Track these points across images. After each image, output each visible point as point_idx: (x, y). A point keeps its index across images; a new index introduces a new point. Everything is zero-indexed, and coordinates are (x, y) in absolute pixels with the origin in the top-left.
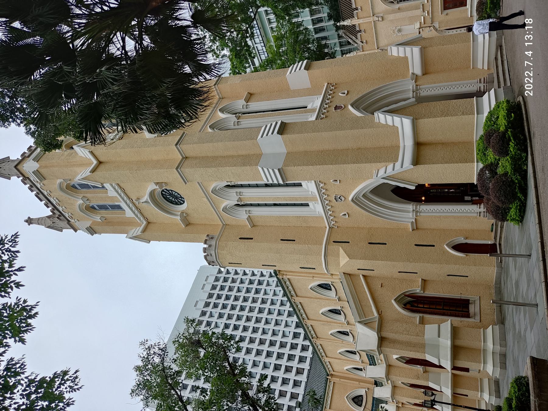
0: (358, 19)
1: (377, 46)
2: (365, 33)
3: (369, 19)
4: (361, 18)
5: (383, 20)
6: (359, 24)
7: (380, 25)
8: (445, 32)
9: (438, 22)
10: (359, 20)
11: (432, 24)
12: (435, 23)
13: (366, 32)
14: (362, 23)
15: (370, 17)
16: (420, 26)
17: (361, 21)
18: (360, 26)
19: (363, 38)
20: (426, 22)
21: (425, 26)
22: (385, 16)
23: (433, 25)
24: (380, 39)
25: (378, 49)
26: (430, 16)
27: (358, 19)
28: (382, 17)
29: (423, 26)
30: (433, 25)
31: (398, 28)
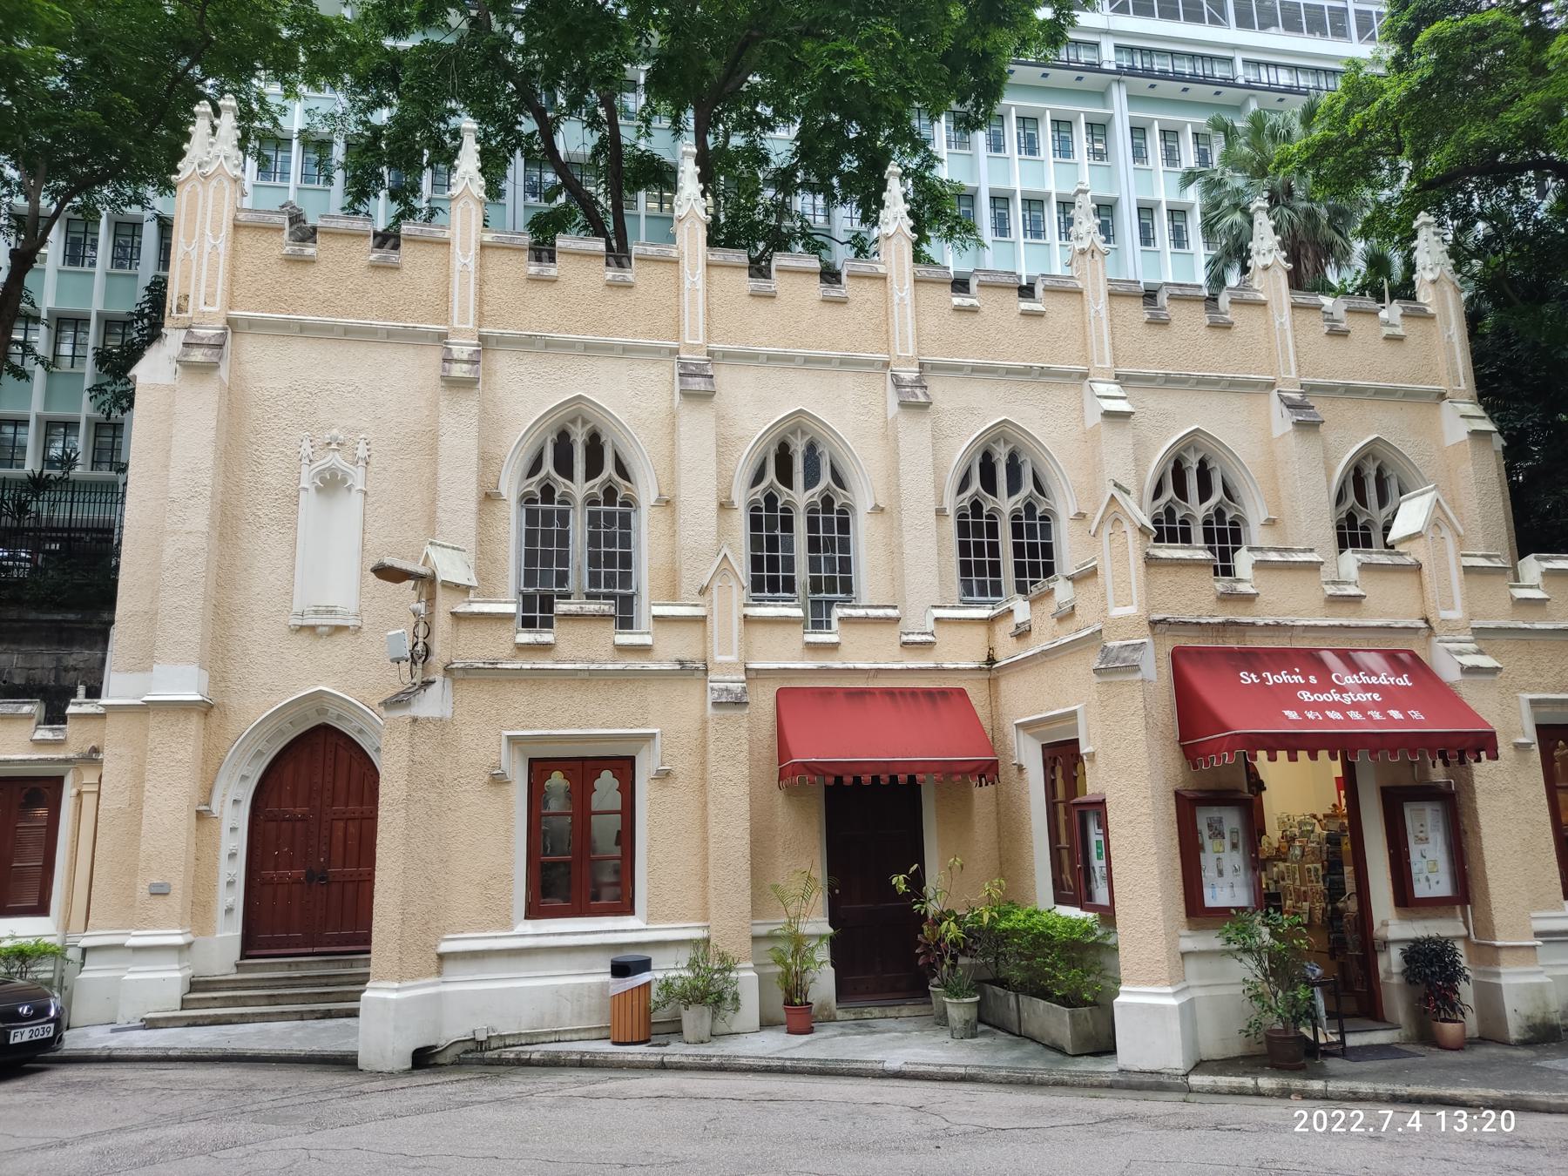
0: (483, 247)
1: (252, 324)
2: (375, 267)
3: (464, 311)
4: (481, 267)
5: (453, 384)
6: (447, 243)
7: (420, 367)
8: (244, 778)
9: (449, 715)
10: (474, 248)
11: (448, 670)
12: (448, 691)
13: (379, 276)
14: (447, 264)
15: (481, 317)
16: (446, 584)
17: (464, 257)
18: (429, 248)
19: (338, 244)
20: (466, 630)
21: (442, 622)
22: (469, 404)
23: (438, 677)
24: (303, 357)
25: (231, 323)
26: (513, 658)
27: (483, 247)
28: (467, 384)
29: (446, 604)
30: (438, 678)
31: (358, 478)
